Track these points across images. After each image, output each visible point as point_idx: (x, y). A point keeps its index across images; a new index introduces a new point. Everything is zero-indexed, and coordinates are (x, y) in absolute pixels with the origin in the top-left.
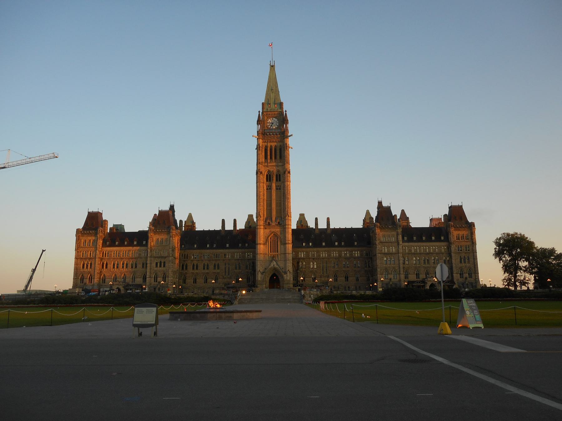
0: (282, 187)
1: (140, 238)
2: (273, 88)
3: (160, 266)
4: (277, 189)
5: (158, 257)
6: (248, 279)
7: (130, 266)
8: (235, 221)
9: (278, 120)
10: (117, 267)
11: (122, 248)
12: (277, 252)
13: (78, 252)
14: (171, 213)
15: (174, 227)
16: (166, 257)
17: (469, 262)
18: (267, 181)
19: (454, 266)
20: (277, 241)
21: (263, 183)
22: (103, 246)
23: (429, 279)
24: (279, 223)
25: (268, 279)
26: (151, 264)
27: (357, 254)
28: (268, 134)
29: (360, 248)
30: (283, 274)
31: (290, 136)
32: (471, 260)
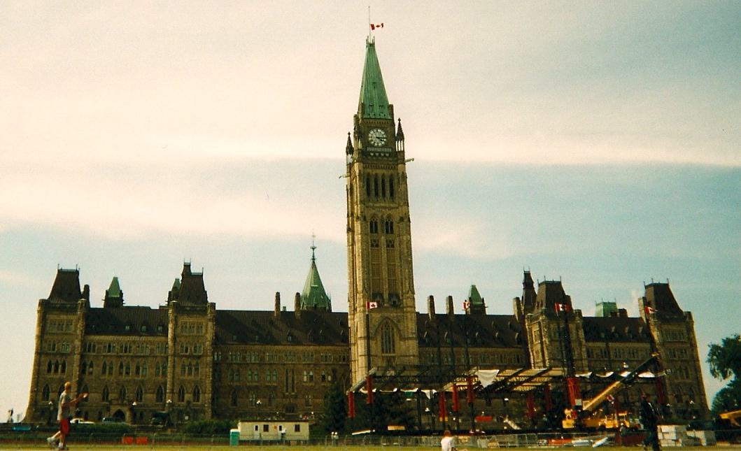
0: (397, 244)
1: (146, 320)
2: (373, 81)
3: (190, 374)
4: (388, 246)
5: (186, 356)
7: (133, 369)
9: (386, 133)
10: (111, 373)
11: (121, 338)
12: (394, 351)
13: (41, 341)
16: (199, 357)
18: (372, 232)
20: (382, 333)
21: (367, 234)
24: (394, 302)
26: (174, 367)
28: (372, 154)
31: (409, 161)
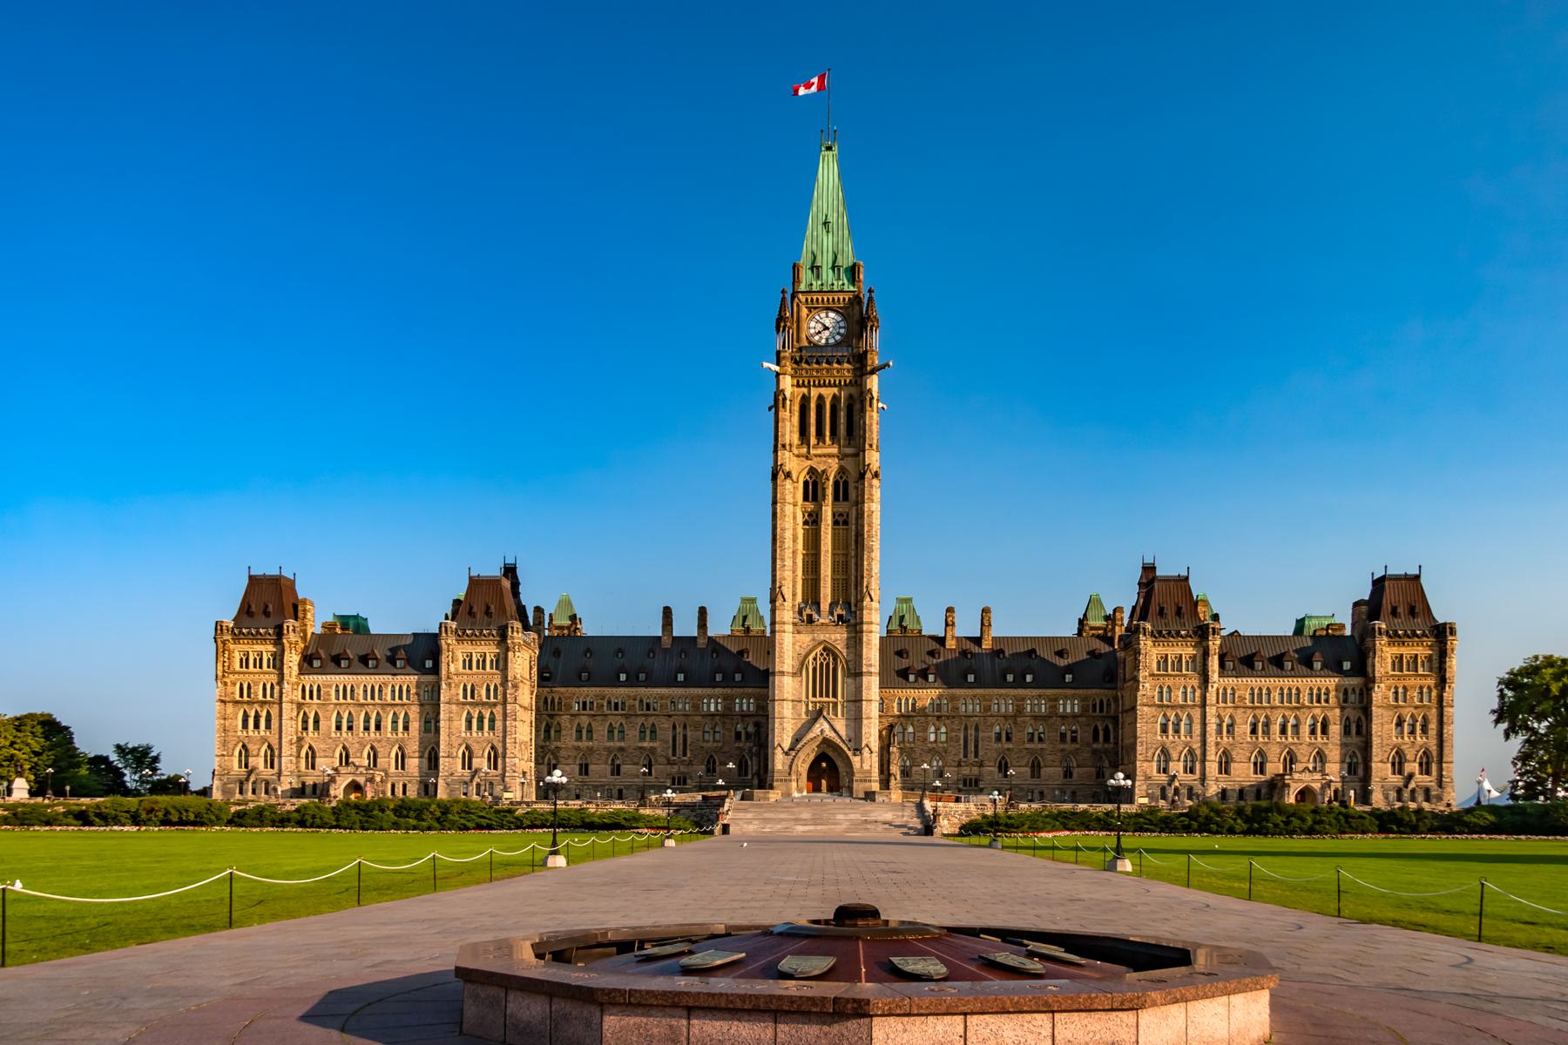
5: (471, 704)
6: (742, 766)
8: (703, 612)
14: (507, 584)
15: (518, 625)
16: (495, 705)
17: (1424, 730)
19: (1376, 741)
22: (301, 672)
23: (1296, 776)
25: (803, 766)
26: (450, 719)
27: (1069, 707)
29: (1081, 692)
30: (850, 754)
32: (1433, 726)
